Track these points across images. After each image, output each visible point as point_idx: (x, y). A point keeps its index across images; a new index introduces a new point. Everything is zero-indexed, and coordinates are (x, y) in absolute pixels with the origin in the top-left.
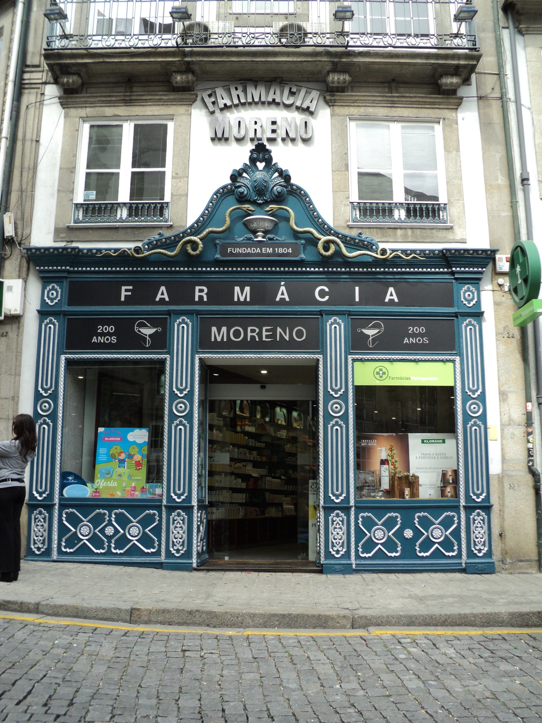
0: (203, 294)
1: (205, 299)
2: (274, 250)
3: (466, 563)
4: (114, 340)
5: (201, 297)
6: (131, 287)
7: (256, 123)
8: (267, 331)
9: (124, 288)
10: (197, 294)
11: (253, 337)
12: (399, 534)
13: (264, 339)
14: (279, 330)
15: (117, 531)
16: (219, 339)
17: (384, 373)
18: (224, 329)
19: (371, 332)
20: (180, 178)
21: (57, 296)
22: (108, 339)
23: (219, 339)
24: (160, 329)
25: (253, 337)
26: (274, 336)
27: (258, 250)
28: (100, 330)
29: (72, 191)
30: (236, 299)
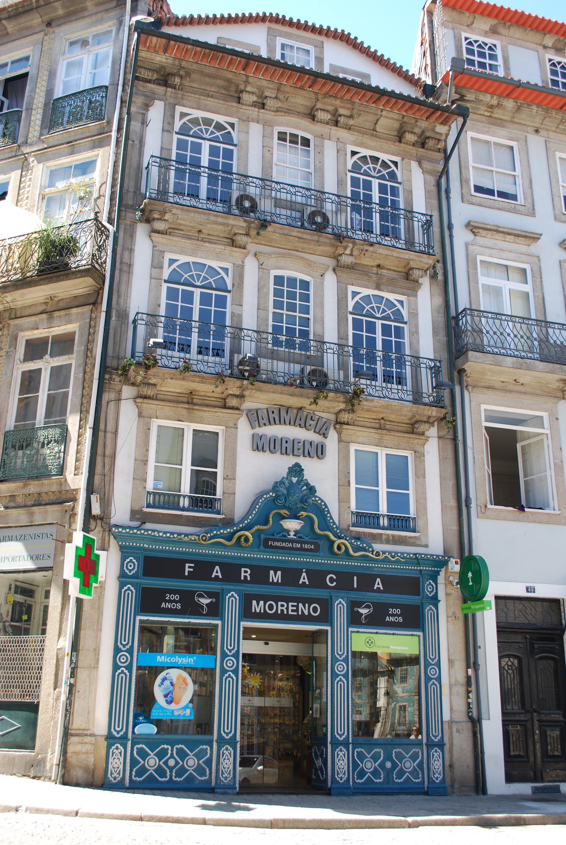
0: (247, 574)
1: (249, 579)
2: (301, 546)
3: (428, 788)
4: (179, 606)
5: (245, 577)
6: (193, 565)
7: (287, 442)
8: (292, 606)
9: (187, 565)
10: (243, 574)
11: (282, 611)
12: (382, 765)
13: (290, 613)
14: (301, 605)
15: (177, 763)
16: (258, 611)
17: (372, 643)
18: (262, 603)
19: (364, 611)
20: (230, 479)
21: (134, 568)
22: (174, 606)
23: (258, 611)
24: (214, 600)
25: (282, 611)
26: (297, 611)
27: (291, 545)
28: (168, 597)
29: (145, 480)
30: (271, 581)
